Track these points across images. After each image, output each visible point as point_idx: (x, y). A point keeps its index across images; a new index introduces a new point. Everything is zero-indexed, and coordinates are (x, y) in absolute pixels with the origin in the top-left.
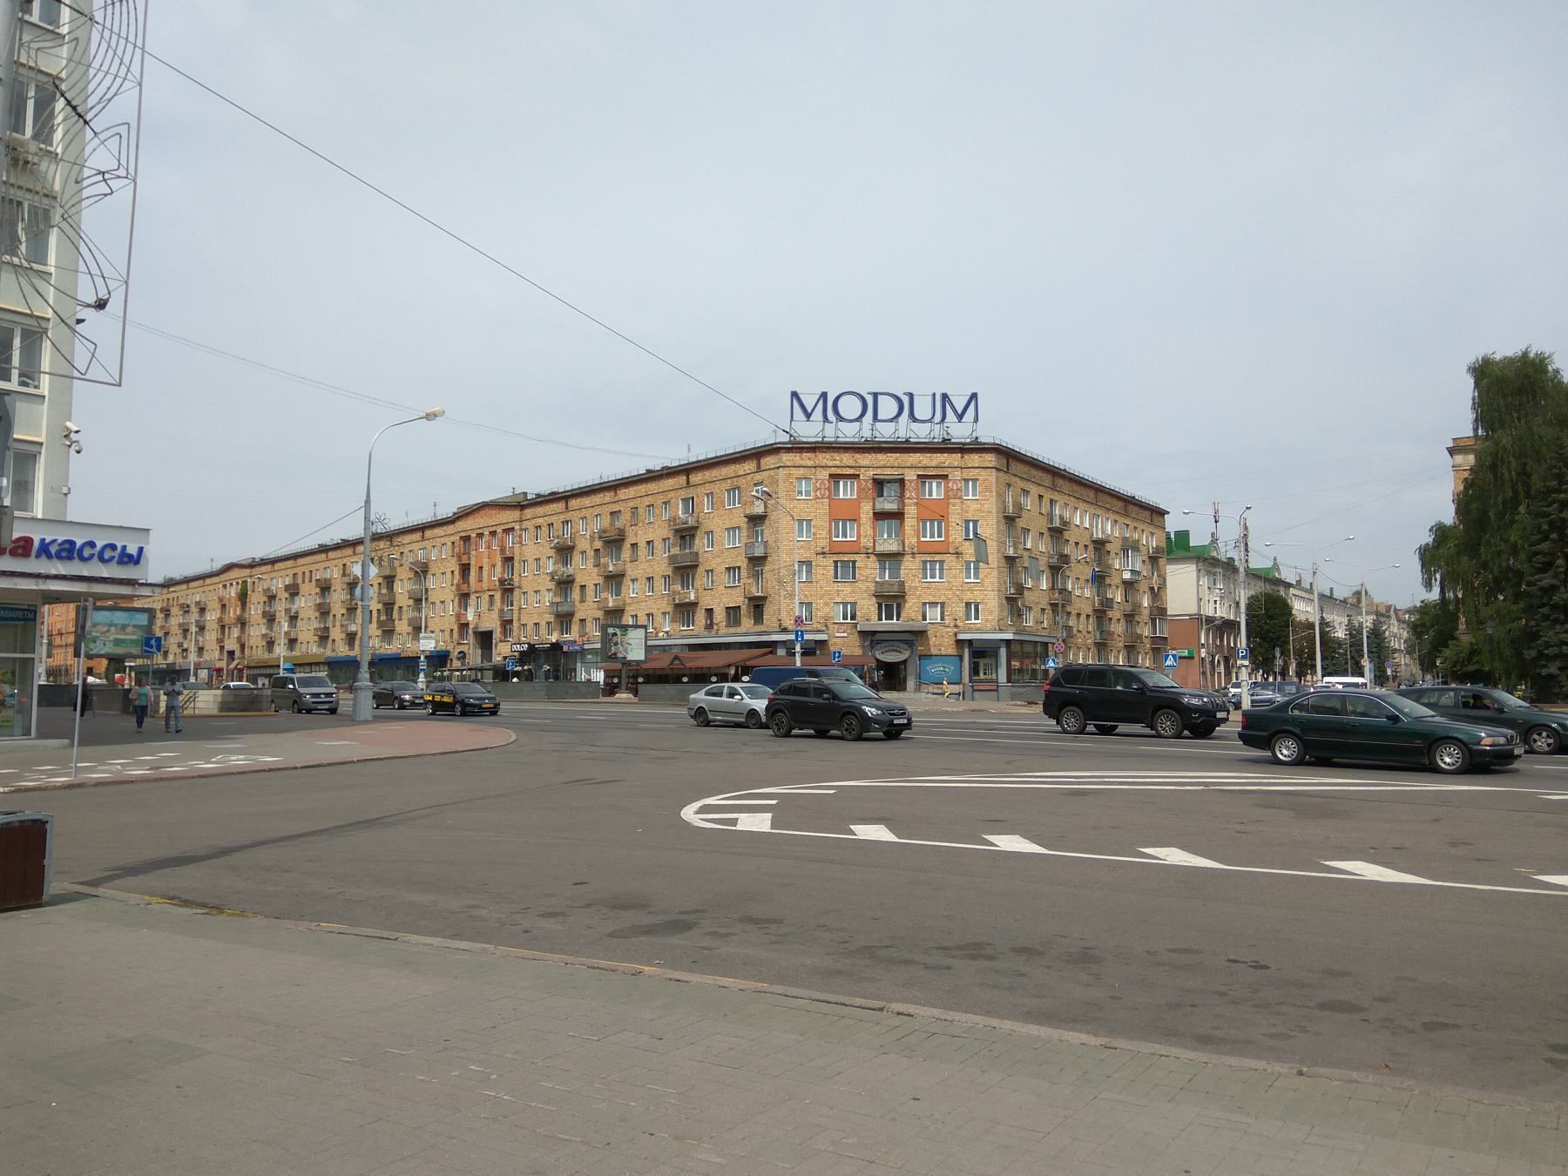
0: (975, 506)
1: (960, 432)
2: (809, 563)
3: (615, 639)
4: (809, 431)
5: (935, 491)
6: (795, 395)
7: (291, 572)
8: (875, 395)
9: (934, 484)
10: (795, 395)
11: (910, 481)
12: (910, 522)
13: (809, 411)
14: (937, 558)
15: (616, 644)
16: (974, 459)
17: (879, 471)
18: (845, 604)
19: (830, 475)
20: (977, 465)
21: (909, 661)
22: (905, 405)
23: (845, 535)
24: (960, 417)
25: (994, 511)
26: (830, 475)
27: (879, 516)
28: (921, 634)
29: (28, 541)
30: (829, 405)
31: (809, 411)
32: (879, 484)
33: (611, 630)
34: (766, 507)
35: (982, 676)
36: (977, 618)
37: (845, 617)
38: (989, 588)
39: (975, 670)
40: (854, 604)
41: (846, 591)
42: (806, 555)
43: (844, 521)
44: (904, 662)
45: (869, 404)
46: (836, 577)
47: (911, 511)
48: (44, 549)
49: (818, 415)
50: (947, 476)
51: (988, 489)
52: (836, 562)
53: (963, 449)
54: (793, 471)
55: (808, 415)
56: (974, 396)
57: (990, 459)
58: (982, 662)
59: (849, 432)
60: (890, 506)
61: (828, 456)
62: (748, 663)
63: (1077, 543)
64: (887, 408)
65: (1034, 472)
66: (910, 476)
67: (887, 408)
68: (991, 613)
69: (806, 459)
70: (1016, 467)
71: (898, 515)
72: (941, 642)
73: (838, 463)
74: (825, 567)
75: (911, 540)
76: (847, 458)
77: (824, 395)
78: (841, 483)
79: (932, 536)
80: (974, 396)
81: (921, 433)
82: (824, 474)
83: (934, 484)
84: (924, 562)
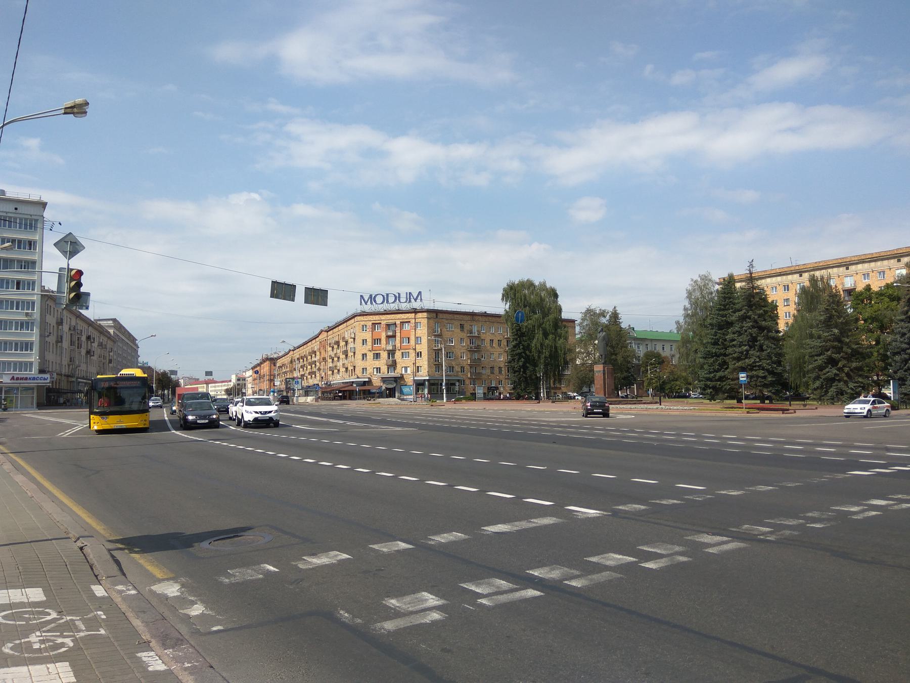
0: (420, 332)
1: (416, 305)
2: (366, 354)
3: (289, 383)
4: (368, 308)
5: (407, 327)
6: (362, 296)
7: (299, 353)
8: (387, 295)
9: (407, 325)
10: (362, 296)
11: (398, 324)
12: (398, 338)
13: (366, 300)
14: (407, 351)
15: (290, 384)
16: (419, 315)
17: (388, 321)
18: (377, 368)
19: (372, 324)
20: (421, 317)
21: (396, 388)
22: (397, 297)
23: (378, 344)
24: (416, 300)
25: (426, 333)
26: (372, 324)
27: (388, 337)
28: (402, 377)
29: (27, 378)
30: (372, 299)
31: (366, 300)
32: (388, 326)
33: (288, 380)
34: (355, 335)
35: (420, 392)
36: (421, 372)
37: (377, 373)
38: (424, 362)
39: (417, 390)
40: (380, 368)
41: (377, 364)
42: (364, 352)
43: (377, 340)
44: (395, 387)
45: (386, 299)
46: (374, 359)
47: (398, 334)
48: (30, 378)
49: (369, 303)
50: (410, 322)
51: (424, 326)
52: (374, 354)
53: (415, 311)
54: (361, 322)
55: (366, 303)
56: (420, 293)
57: (425, 315)
58: (420, 387)
59: (382, 308)
60: (390, 333)
61: (371, 317)
62: (342, 389)
63: (492, 341)
64: (391, 299)
65: (456, 316)
66: (398, 322)
67: (391, 299)
68: (425, 369)
69: (365, 318)
70: (440, 316)
71: (394, 336)
72: (409, 380)
73: (374, 319)
74: (370, 356)
75: (398, 345)
76: (377, 317)
77: (371, 296)
78: (376, 326)
79: (406, 343)
80: (420, 293)
81: (404, 306)
82: (370, 323)
83: (407, 325)
84: (402, 353)
